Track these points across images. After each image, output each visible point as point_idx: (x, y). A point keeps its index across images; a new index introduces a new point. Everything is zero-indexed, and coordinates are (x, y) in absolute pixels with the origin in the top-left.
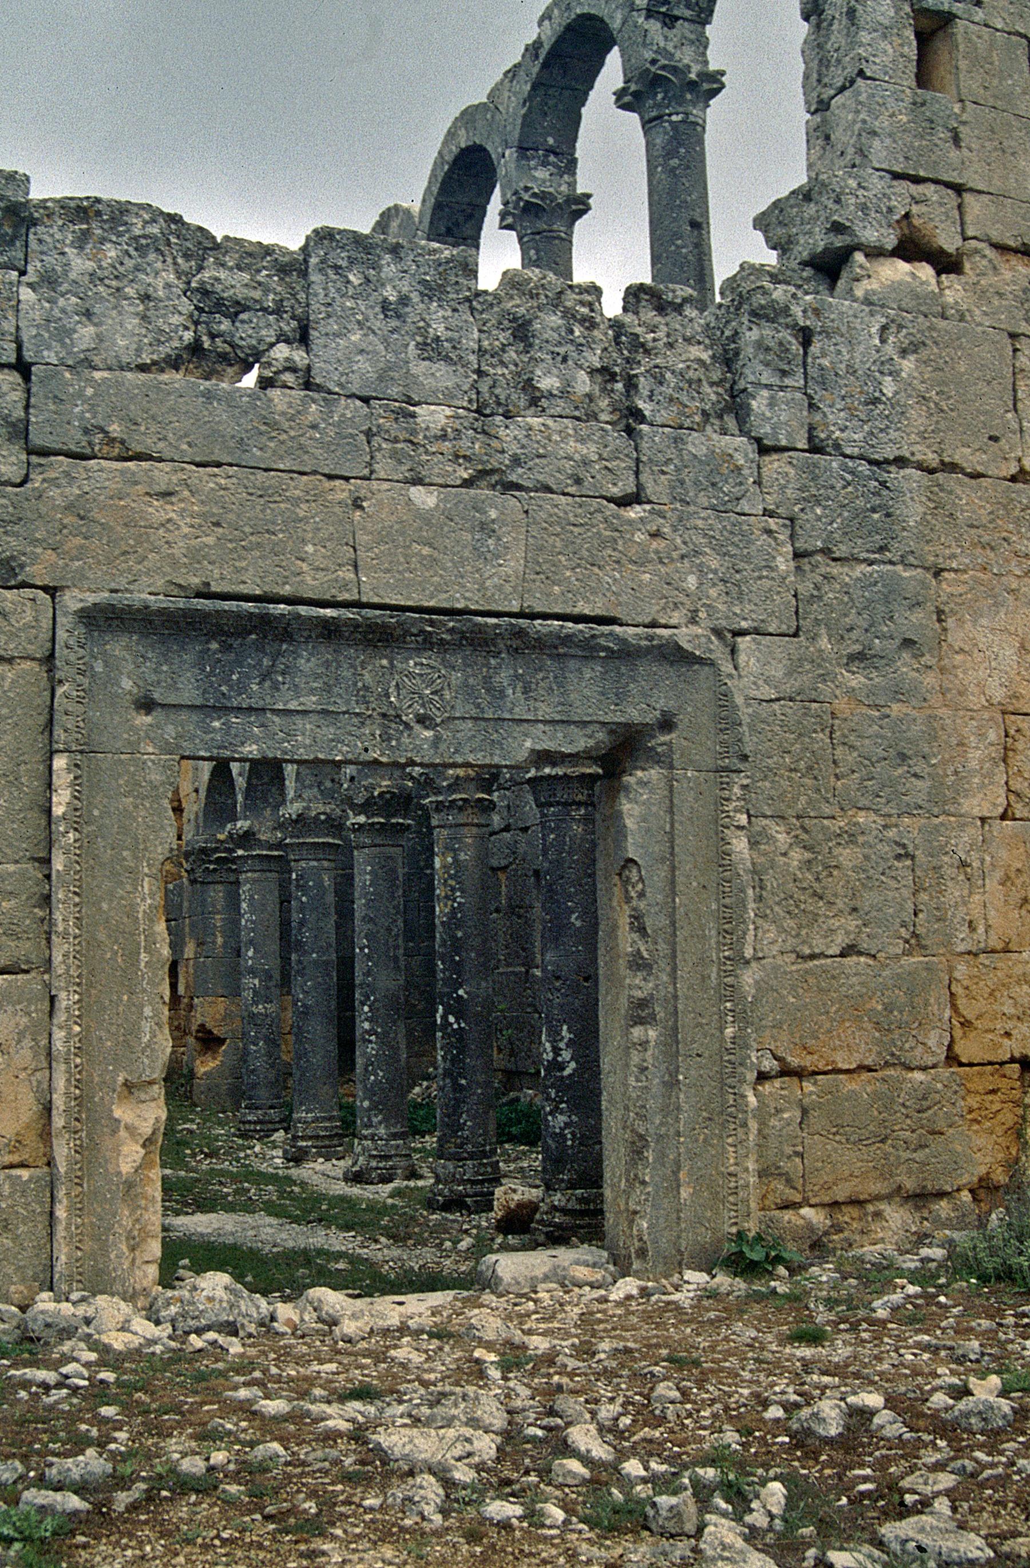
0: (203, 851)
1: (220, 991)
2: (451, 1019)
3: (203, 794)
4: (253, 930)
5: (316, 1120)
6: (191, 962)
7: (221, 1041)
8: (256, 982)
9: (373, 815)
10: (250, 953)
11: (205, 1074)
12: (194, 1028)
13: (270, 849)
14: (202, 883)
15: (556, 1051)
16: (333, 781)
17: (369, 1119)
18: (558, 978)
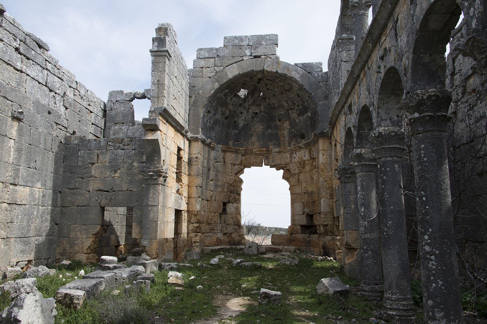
0: (344, 169)
1: (354, 228)
3: (343, 146)
4: (363, 199)
5: (397, 300)
6: (342, 216)
7: (354, 249)
8: (366, 223)
9: (423, 112)
10: (363, 210)
11: (348, 263)
12: (344, 243)
13: (369, 162)
14: (344, 183)
16: (398, 116)
17: (433, 314)
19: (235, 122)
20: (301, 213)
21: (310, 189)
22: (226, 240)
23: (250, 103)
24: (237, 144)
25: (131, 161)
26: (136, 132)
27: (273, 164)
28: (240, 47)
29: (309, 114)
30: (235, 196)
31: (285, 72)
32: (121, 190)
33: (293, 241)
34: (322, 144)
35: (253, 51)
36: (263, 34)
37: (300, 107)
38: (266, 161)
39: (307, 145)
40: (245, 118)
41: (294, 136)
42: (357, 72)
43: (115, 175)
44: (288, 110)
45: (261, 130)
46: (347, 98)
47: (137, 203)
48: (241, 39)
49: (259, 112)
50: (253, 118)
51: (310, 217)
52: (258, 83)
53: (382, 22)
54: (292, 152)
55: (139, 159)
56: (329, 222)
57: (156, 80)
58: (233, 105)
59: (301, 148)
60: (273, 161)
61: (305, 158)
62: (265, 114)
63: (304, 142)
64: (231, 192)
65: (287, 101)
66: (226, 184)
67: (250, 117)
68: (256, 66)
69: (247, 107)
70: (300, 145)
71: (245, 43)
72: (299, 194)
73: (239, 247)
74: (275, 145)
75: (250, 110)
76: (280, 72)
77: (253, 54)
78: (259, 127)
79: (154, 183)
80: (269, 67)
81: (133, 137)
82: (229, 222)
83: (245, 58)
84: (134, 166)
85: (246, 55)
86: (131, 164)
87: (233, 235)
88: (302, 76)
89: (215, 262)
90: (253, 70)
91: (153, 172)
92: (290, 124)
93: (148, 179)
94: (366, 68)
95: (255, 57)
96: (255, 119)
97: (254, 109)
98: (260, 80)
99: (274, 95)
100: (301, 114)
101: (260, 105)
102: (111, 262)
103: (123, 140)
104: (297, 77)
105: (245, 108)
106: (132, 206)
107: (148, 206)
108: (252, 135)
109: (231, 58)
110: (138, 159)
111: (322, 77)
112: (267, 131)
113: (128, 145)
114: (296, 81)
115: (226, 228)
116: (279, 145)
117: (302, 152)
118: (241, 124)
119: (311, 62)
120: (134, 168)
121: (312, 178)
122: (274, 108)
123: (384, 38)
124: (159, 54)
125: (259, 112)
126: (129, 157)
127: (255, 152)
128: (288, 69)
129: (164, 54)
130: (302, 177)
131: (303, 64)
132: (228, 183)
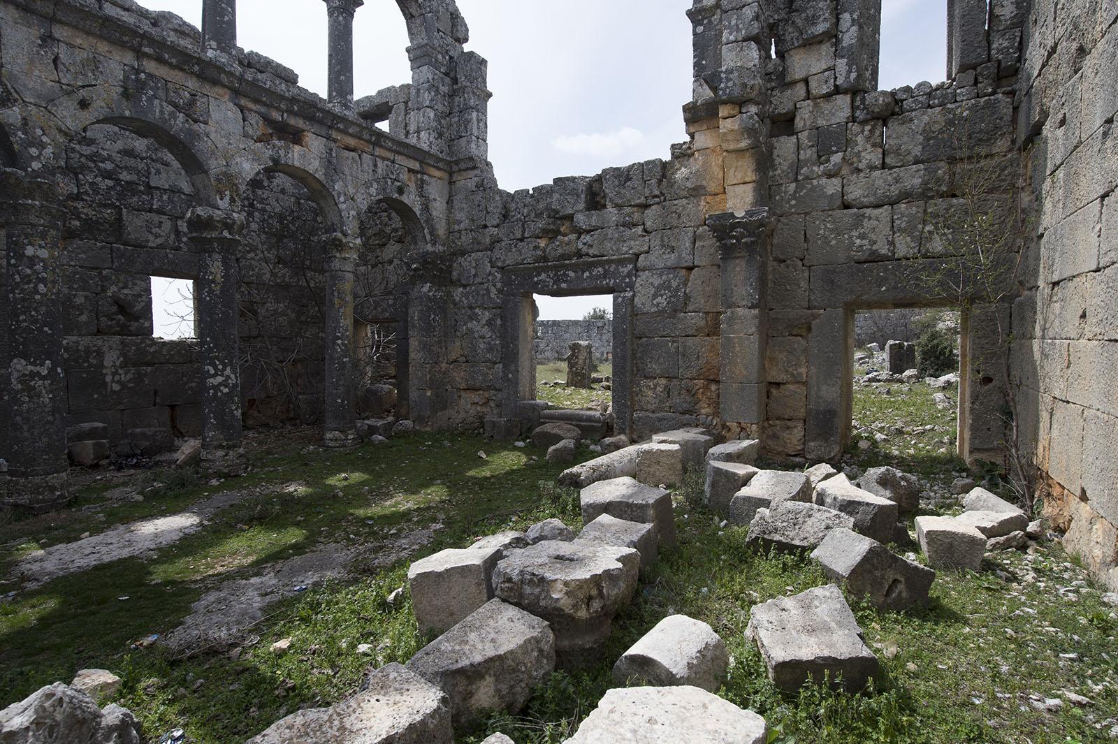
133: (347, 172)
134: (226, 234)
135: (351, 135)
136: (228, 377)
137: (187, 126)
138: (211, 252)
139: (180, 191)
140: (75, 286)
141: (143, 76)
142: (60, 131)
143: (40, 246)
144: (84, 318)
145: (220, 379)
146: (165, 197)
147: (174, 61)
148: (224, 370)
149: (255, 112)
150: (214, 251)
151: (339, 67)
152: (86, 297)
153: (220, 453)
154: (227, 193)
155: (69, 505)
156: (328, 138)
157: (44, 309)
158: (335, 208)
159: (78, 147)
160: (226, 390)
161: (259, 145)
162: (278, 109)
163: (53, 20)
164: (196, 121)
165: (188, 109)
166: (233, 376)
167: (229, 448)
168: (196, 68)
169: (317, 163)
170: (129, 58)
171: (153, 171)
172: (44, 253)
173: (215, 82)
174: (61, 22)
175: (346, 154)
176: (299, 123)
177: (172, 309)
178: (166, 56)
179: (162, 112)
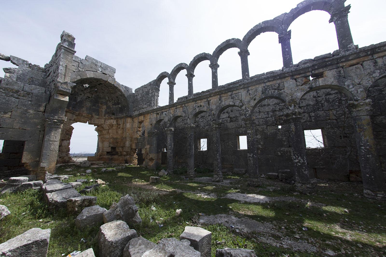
2: (255, 156)
15: (304, 161)
18: (302, 149)
19: (76, 98)
20: (108, 146)
21: (115, 137)
22: (61, 161)
23: (87, 92)
24: (74, 109)
25: (26, 108)
26: (34, 89)
27: (93, 123)
28: (96, 65)
29: (120, 106)
30: (69, 137)
31: (118, 86)
32: (11, 127)
33: (102, 159)
34: (129, 120)
35: (103, 70)
36: (109, 65)
37: (115, 102)
38: (90, 121)
39: (117, 119)
40: (82, 98)
41: (108, 113)
42: (177, 105)
43: (4, 116)
44: (107, 101)
45: (89, 106)
46: (163, 109)
47: (30, 138)
48: (97, 61)
49: (91, 97)
50: (86, 99)
51: (113, 148)
52: (99, 85)
53: (202, 98)
54: (105, 119)
55: (36, 109)
56: (129, 150)
57: (65, 65)
58: (78, 89)
59: (112, 119)
60: (94, 122)
61: (113, 123)
62: (94, 99)
63: (113, 117)
64: (67, 134)
65: (108, 97)
66: (65, 130)
67: (85, 98)
68: (104, 78)
69: (85, 93)
70: (112, 117)
71: (99, 65)
72: (108, 138)
73: (69, 164)
74: (96, 114)
75: (86, 95)
76: (115, 85)
77: (104, 72)
78: (88, 104)
79: (56, 127)
80: (110, 80)
81: (30, 92)
82: (63, 151)
83: (98, 71)
84: (29, 112)
85: (99, 70)
86: (26, 111)
87: (65, 158)
88: (124, 91)
89: (89, 171)
90: (102, 79)
91: (57, 120)
92: (107, 107)
93: (52, 124)
94: (184, 105)
95: (103, 73)
96: (87, 100)
97: (89, 95)
98: (101, 84)
99: (103, 93)
100: (115, 104)
101: (92, 94)
102: (24, 181)
103: (17, 92)
104: (123, 91)
105: (84, 93)
106: (24, 140)
107: (49, 140)
108: (83, 107)
109: (90, 68)
110: (34, 108)
111: (132, 94)
112: (92, 107)
113: (23, 96)
114: (121, 92)
115: (62, 154)
116: (98, 115)
117: (112, 121)
118: (79, 100)
119: (129, 87)
120: (29, 113)
121: (117, 132)
122: (100, 98)
123: (199, 102)
124: (68, 50)
125: (91, 97)
126: (25, 105)
127: (84, 115)
128: (119, 86)
129: (73, 52)
130: (110, 131)
131: (125, 86)
132: (66, 129)
133: (353, 74)
134: (294, 116)
135: (352, 60)
136: (300, 160)
137: (278, 92)
138: (291, 122)
139: (310, 105)
140: (283, 136)
141: (266, 87)
142: (251, 107)
143: (250, 130)
144: (285, 143)
145: (297, 161)
146: (305, 108)
147: (272, 79)
148: (298, 157)
149: (301, 77)
150: (291, 122)
151: (341, 39)
152: (286, 138)
153: (300, 185)
154: (293, 105)
155: (257, 187)
156: (338, 68)
157: (251, 143)
158: (348, 91)
159: (281, 104)
160: (300, 164)
161: (303, 86)
162: (309, 72)
163: (248, 87)
164: (281, 90)
165: (279, 89)
166: (302, 160)
167: (303, 184)
168: (278, 77)
169: (333, 79)
170: (263, 85)
171: (300, 102)
172: (250, 132)
173: (285, 77)
174: (250, 86)
175: (351, 68)
176: (321, 70)
177: (243, 143)
178: (270, 79)
179: (271, 92)
